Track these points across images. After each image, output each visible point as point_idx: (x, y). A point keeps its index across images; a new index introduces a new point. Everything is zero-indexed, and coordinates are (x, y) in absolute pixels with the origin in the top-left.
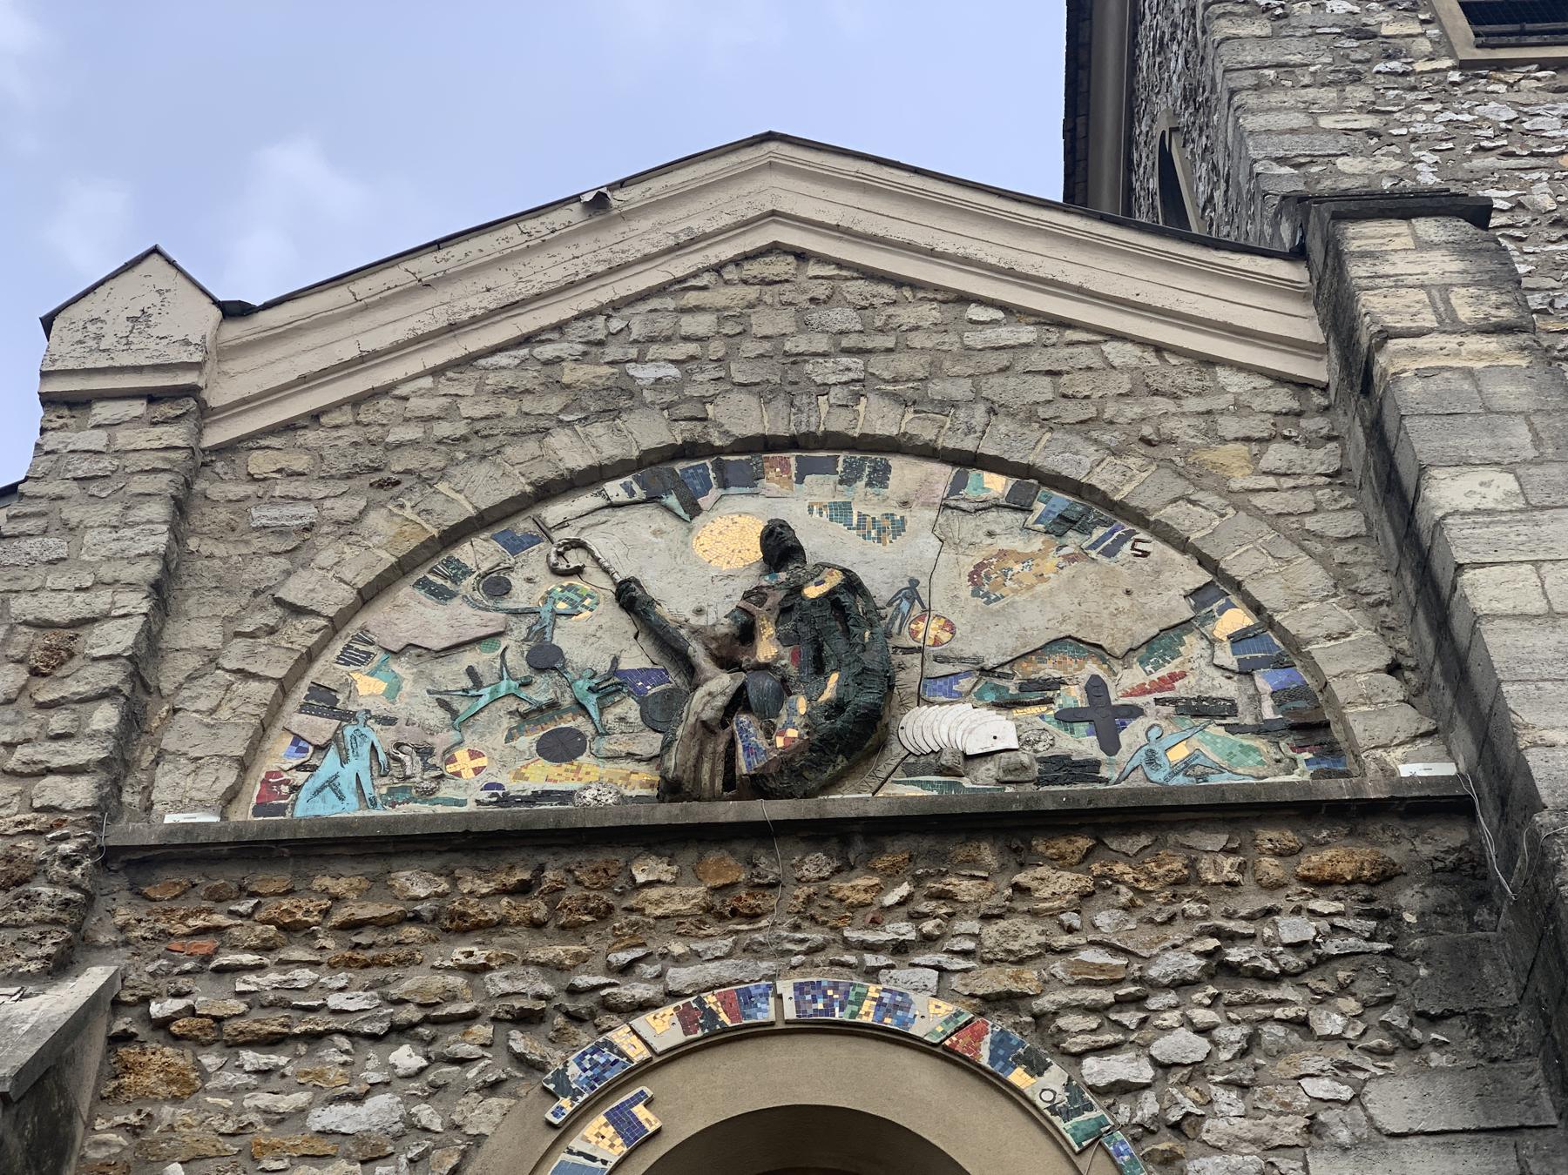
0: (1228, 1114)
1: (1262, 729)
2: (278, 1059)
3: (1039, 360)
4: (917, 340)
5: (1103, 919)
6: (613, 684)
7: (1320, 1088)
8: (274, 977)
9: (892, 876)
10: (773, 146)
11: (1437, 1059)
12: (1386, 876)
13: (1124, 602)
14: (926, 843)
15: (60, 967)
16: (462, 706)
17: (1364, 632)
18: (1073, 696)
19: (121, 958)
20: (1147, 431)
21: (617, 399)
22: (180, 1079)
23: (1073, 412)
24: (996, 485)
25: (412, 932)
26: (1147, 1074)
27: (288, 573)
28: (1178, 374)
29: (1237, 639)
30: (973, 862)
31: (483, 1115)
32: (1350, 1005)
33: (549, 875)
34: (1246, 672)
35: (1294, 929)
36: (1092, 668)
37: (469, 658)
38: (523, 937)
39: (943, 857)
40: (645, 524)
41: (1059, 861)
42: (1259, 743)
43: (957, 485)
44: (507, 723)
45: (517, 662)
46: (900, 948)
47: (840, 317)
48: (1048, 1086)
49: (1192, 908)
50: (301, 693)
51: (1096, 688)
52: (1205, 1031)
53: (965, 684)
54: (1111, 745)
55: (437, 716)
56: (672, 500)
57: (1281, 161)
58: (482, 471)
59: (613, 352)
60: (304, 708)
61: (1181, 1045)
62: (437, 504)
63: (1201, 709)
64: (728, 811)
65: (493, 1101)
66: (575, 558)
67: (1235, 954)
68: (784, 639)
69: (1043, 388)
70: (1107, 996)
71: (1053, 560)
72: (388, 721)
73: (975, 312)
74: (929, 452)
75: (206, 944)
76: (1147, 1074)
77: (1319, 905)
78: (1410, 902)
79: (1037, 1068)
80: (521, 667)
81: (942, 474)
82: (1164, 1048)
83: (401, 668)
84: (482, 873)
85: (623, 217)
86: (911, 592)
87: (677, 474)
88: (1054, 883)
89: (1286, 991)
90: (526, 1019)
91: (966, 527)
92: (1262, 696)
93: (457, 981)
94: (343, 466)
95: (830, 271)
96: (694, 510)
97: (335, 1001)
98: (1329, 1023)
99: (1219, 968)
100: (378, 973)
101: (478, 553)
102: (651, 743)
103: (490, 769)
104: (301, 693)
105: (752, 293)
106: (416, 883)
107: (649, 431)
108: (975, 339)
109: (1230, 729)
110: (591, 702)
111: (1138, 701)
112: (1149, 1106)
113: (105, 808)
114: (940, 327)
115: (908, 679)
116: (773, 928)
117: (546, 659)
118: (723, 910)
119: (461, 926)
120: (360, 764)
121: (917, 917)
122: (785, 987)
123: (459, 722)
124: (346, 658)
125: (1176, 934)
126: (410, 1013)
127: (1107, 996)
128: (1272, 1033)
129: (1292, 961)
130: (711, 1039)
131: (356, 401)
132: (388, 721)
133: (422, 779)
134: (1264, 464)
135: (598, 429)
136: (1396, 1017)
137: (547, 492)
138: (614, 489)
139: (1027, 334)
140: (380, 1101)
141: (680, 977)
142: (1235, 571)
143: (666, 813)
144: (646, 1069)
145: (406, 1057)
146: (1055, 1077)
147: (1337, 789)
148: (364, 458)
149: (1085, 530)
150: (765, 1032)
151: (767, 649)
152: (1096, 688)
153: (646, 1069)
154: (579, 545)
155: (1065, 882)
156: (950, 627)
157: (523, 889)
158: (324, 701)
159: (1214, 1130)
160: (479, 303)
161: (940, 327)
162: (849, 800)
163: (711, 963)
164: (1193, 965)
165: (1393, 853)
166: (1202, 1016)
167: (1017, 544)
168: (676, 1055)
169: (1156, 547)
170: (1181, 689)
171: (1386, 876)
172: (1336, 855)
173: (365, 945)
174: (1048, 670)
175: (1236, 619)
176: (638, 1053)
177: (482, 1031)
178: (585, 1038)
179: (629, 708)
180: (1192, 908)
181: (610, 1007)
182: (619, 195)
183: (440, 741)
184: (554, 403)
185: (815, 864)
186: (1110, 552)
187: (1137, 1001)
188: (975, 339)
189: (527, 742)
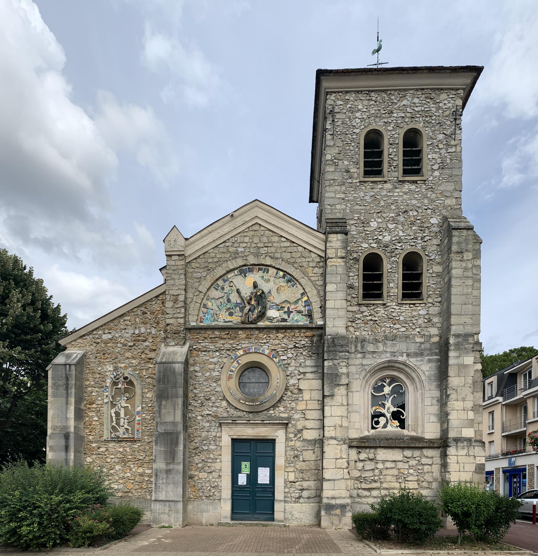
0: (293, 363)
1: (305, 315)
2: (206, 353)
3: (289, 250)
4: (275, 245)
5: (285, 340)
6: (237, 305)
7: (302, 361)
8: (204, 344)
9: (264, 334)
10: (257, 202)
11: (313, 358)
12: (314, 336)
13: (293, 295)
14: (268, 330)
15: (184, 344)
16: (220, 307)
17: (319, 302)
18: (286, 309)
19: (189, 341)
20: (301, 265)
21: (236, 255)
22: (197, 355)
23: (292, 260)
24: (281, 274)
25: (217, 339)
26: (286, 358)
27: (199, 285)
28: (307, 254)
29: (305, 301)
30: (273, 333)
31: (225, 360)
32: (306, 351)
33: (230, 333)
34: (305, 306)
35: (303, 342)
36: (289, 305)
37: (221, 300)
38: (228, 340)
39: (270, 332)
40: (240, 278)
41: (282, 333)
42: (304, 317)
43: (277, 274)
44: (225, 310)
45: (226, 301)
46: (265, 343)
47: (265, 239)
48: (276, 360)
49: (294, 339)
50: (202, 305)
51: (288, 308)
52: (292, 354)
53: (274, 307)
54: (289, 317)
55: (217, 309)
56: (243, 275)
57: (329, 205)
58: (220, 268)
59: (236, 245)
60: (203, 307)
61: (290, 355)
62: (215, 274)
63: (299, 312)
64: (248, 326)
65: (226, 359)
66: (232, 284)
67: (297, 345)
68: (255, 301)
69: (289, 256)
70: (283, 350)
71: (287, 287)
72: (212, 310)
73: (283, 239)
74: (274, 267)
75: (197, 339)
76: (286, 358)
77: (306, 340)
78: (315, 339)
79: (276, 358)
80: (226, 302)
81: (275, 271)
82: (288, 356)
83: (213, 301)
84: (224, 332)
85: (236, 218)
86: (270, 292)
87: (244, 270)
88: (281, 335)
89: (301, 350)
90: (228, 350)
91: (277, 281)
92: (305, 310)
93: (222, 345)
94: (203, 266)
95: (263, 229)
96: (245, 276)
97: (211, 347)
98: (304, 353)
99: (295, 347)
100: (214, 344)
101: (220, 282)
102: (240, 314)
103: (224, 319)
104: (202, 305)
105: (253, 233)
106: (217, 333)
107: (240, 262)
108: (283, 245)
109: (302, 315)
110: (234, 307)
111: (293, 310)
112: (286, 362)
113: (185, 323)
114: (278, 242)
115: (268, 306)
116: (252, 340)
117: (229, 301)
118: (248, 338)
119: (222, 338)
120: (210, 316)
121: (267, 339)
122: (253, 348)
123: (220, 310)
124: (207, 300)
125: (292, 342)
126: (218, 349)
127: (283, 350)
128: (299, 354)
129: (302, 346)
130: (246, 353)
131: (204, 254)
132: (212, 310)
133: (216, 318)
134: (314, 272)
135: (234, 261)
136: (310, 353)
137: (228, 272)
138: (236, 272)
139: (288, 244)
140: (216, 358)
141: (243, 346)
142: (307, 291)
143: (242, 326)
144: (240, 356)
145: (218, 354)
146: (277, 359)
147: (310, 326)
148: (206, 264)
149: (291, 282)
150: (251, 353)
151: (253, 302)
152: (288, 308)
153: (240, 356)
154: (232, 282)
155: (282, 335)
156: (274, 297)
157: (228, 334)
158: (205, 306)
159: (291, 365)
160: (218, 236)
161: (278, 242)
162: (261, 324)
163: (245, 344)
164: (292, 346)
165: (314, 333)
166: (292, 352)
167: (282, 284)
168: (243, 355)
169: (298, 286)
170: (298, 309)
171: (314, 336)
172: (309, 334)
173: (213, 340)
174: (284, 305)
175: (305, 298)
176: (239, 355)
177: (224, 351)
178: (234, 352)
179: (238, 309)
180: (294, 339)
181: (236, 349)
182: (235, 213)
183: (218, 313)
184: (228, 255)
185: (257, 332)
186: (293, 286)
187: (287, 350)
188: (283, 245)
189: (227, 313)
